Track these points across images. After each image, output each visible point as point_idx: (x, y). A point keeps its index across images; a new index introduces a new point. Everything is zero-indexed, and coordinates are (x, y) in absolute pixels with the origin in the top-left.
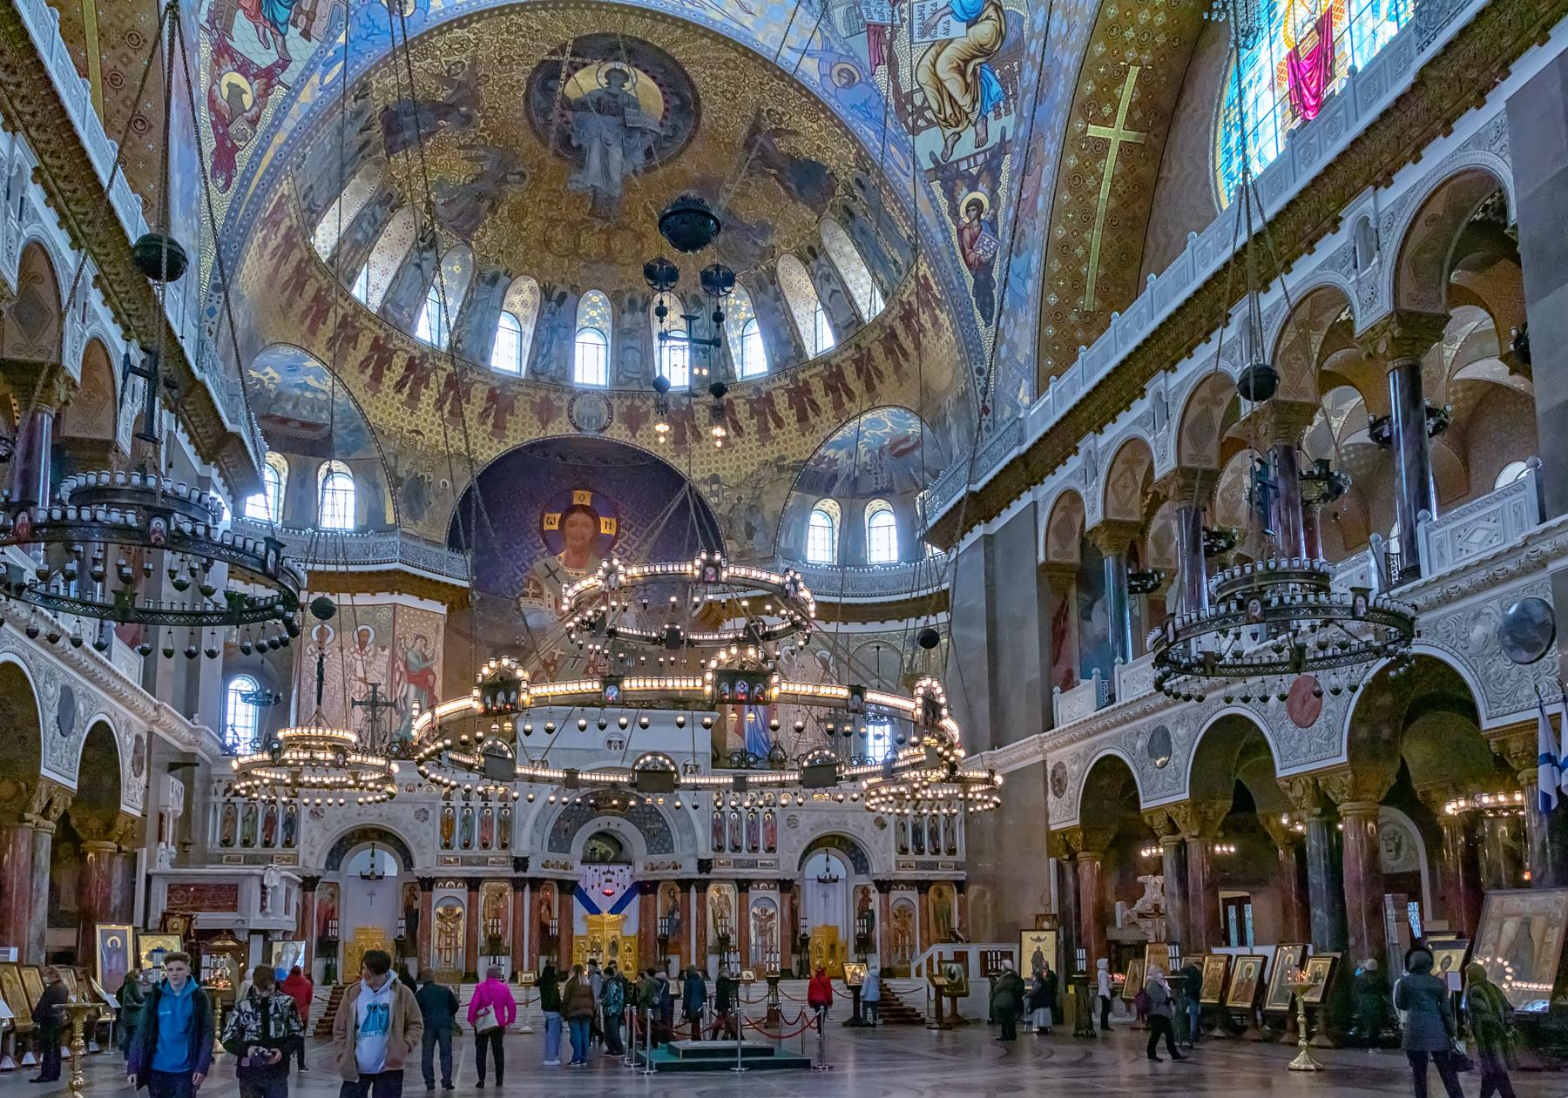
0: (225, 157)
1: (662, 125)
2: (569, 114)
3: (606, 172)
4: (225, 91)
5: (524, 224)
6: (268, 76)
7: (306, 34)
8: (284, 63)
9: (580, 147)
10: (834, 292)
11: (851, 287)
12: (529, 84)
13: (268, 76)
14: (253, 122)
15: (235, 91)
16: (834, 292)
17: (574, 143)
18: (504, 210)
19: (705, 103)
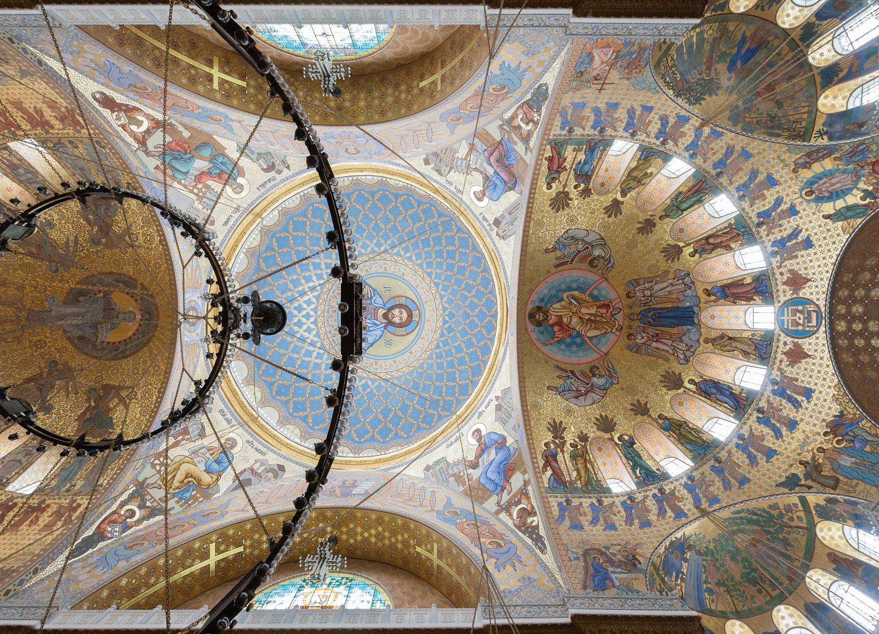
0: (108, 103)
1: (103, 342)
2: (101, 295)
3: (63, 317)
4: (140, 118)
5: (20, 272)
6: (142, 142)
7: (157, 168)
8: (147, 153)
9: (80, 302)
10: (19, 461)
11: (29, 470)
12: (120, 274)
13: (142, 142)
14: (123, 127)
15: (139, 124)
16: (19, 461)
17: (81, 299)
18: (29, 260)
19: (125, 361)
